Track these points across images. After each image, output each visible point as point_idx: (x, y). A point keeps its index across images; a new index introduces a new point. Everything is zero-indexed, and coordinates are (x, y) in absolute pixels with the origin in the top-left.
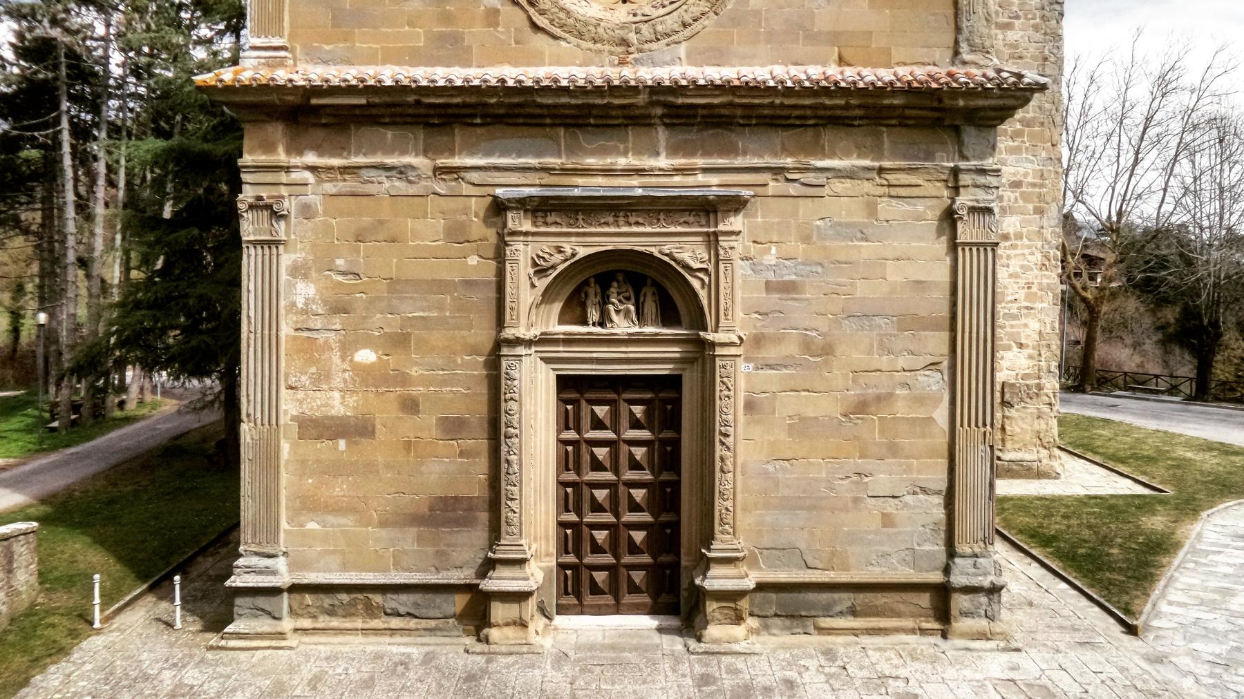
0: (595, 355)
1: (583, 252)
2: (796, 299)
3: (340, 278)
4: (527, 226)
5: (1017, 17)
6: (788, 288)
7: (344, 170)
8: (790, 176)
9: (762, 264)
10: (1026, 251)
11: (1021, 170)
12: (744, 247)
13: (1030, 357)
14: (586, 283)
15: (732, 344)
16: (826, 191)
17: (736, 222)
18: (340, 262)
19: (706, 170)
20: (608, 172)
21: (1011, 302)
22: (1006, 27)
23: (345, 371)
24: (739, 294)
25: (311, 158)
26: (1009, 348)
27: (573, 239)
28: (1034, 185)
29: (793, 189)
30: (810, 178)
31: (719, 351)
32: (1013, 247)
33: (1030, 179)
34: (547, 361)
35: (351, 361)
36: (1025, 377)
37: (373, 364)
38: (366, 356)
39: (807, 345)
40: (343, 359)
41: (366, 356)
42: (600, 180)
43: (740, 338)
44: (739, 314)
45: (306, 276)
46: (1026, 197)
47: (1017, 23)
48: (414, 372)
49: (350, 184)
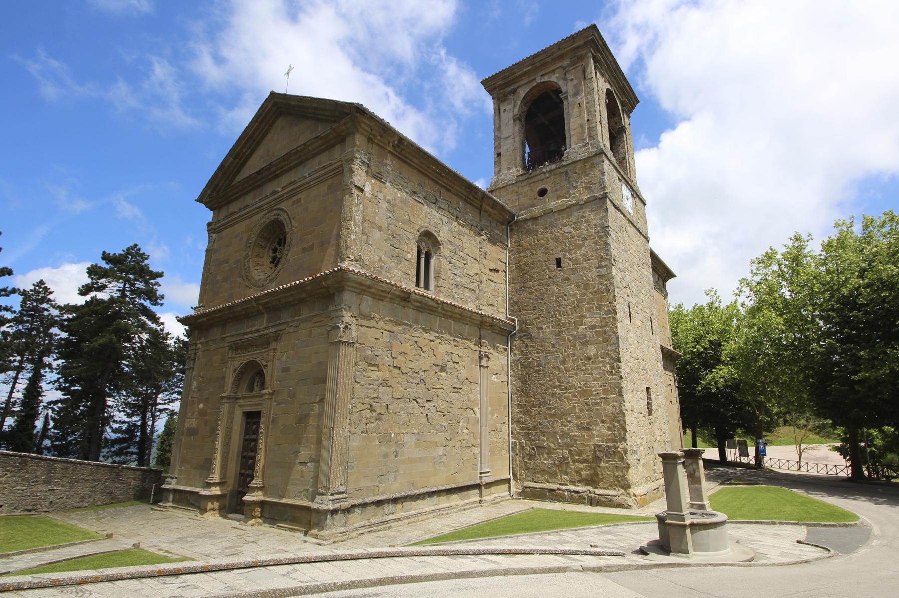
5: (586, 239)
10: (601, 365)
11: (595, 320)
13: (609, 429)
19: (272, 326)
20: (251, 332)
21: (595, 395)
22: (580, 246)
26: (596, 424)
28: (602, 327)
32: (594, 363)
33: (599, 324)
36: (608, 441)
42: (250, 336)
46: (598, 334)
47: (586, 243)
48: (208, 411)
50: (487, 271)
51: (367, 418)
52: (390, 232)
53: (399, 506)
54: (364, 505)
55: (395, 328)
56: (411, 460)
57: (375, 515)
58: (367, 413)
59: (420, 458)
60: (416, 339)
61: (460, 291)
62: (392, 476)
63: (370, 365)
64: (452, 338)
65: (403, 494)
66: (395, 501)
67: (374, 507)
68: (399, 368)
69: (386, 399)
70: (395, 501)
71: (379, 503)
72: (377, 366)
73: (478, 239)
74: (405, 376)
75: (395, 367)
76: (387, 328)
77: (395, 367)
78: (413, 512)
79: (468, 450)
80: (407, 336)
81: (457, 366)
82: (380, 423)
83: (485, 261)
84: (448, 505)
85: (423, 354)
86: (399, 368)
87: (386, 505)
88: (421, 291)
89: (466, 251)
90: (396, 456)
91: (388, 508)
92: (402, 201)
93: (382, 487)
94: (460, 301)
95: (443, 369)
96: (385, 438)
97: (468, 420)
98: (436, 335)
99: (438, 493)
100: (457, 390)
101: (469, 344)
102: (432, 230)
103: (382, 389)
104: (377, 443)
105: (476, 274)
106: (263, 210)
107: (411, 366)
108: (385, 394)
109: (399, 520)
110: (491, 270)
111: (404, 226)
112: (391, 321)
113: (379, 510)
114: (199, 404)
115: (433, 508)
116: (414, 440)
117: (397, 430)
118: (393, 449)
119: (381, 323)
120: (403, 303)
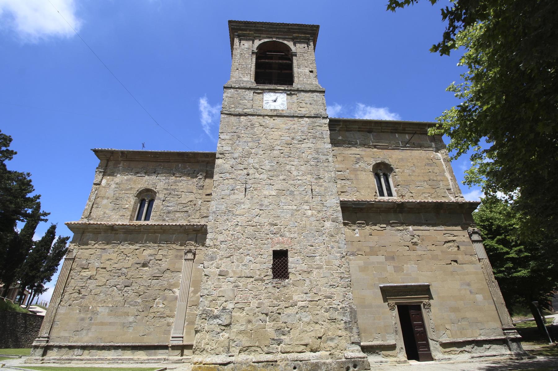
50: (204, 196)
51: (74, 298)
52: (114, 198)
53: (86, 352)
54: (60, 347)
55: (106, 247)
56: (102, 324)
57: (67, 354)
58: (76, 295)
59: (110, 323)
60: (122, 250)
61: (171, 215)
62: (84, 332)
63: (83, 268)
64: (156, 245)
65: (90, 344)
66: (84, 348)
67: (67, 349)
68: (105, 268)
69: (91, 287)
70: (84, 348)
71: (71, 347)
72: (88, 268)
73: (195, 180)
74: (109, 273)
75: (102, 268)
76: (100, 247)
77: (102, 268)
78: (96, 357)
79: (163, 320)
80: (116, 250)
81: (159, 262)
82: (83, 300)
83: (200, 191)
84: (131, 357)
85: (127, 258)
86: (105, 268)
87: (76, 350)
88: (142, 222)
89: (182, 190)
90: (91, 320)
91: (77, 352)
92: (127, 180)
93: (76, 338)
94: (170, 221)
95: (144, 265)
96: (85, 309)
97: (165, 299)
98: (141, 245)
99: (124, 348)
100: (157, 278)
101: (174, 246)
102: (150, 187)
103: (89, 281)
104: (78, 311)
105: (191, 201)
107: (115, 266)
108: (92, 284)
109: (81, 360)
110: (207, 195)
111: (126, 192)
112: (103, 243)
113: (71, 352)
115: (115, 357)
116: (107, 311)
117: (95, 304)
118: (89, 316)
119: (96, 246)
120: (114, 232)
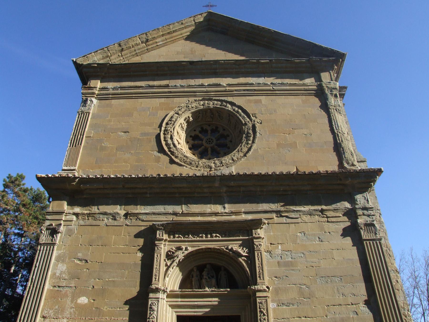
0: (196, 303)
1: (190, 249)
2: (293, 270)
3: (79, 262)
4: (165, 237)
6: (287, 264)
7: (89, 215)
8: (283, 214)
9: (275, 254)
12: (266, 246)
14: (192, 270)
15: (264, 291)
16: (299, 220)
17: (261, 232)
18: (80, 255)
20: (203, 214)
23: (71, 308)
24: (265, 268)
25: (77, 210)
27: (187, 243)
29: (284, 220)
30: (293, 215)
31: (258, 294)
34: (173, 307)
35: (76, 302)
37: (86, 304)
38: (83, 300)
39: (301, 293)
40: (72, 301)
41: (83, 300)
43: (268, 287)
44: (266, 278)
45: (63, 261)
48: (105, 309)
49: (91, 221)
106: (195, 96)
114: (75, 297)
